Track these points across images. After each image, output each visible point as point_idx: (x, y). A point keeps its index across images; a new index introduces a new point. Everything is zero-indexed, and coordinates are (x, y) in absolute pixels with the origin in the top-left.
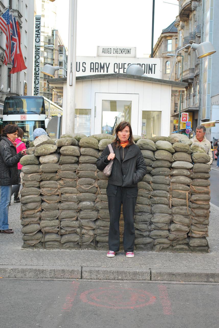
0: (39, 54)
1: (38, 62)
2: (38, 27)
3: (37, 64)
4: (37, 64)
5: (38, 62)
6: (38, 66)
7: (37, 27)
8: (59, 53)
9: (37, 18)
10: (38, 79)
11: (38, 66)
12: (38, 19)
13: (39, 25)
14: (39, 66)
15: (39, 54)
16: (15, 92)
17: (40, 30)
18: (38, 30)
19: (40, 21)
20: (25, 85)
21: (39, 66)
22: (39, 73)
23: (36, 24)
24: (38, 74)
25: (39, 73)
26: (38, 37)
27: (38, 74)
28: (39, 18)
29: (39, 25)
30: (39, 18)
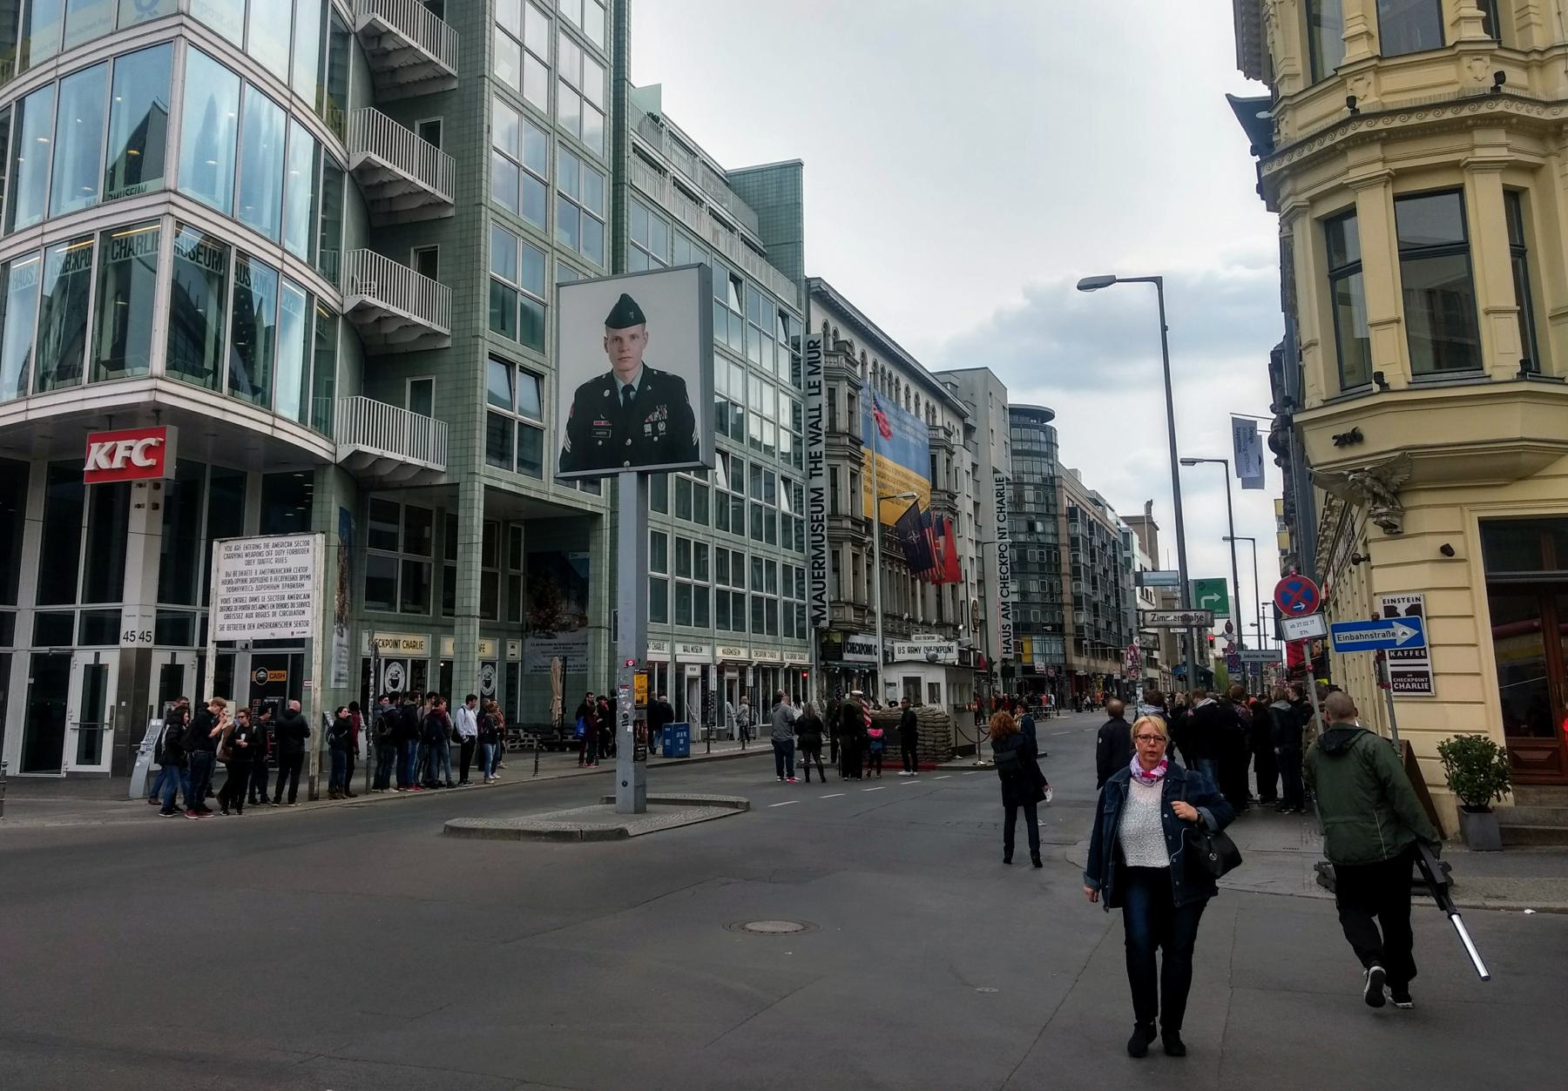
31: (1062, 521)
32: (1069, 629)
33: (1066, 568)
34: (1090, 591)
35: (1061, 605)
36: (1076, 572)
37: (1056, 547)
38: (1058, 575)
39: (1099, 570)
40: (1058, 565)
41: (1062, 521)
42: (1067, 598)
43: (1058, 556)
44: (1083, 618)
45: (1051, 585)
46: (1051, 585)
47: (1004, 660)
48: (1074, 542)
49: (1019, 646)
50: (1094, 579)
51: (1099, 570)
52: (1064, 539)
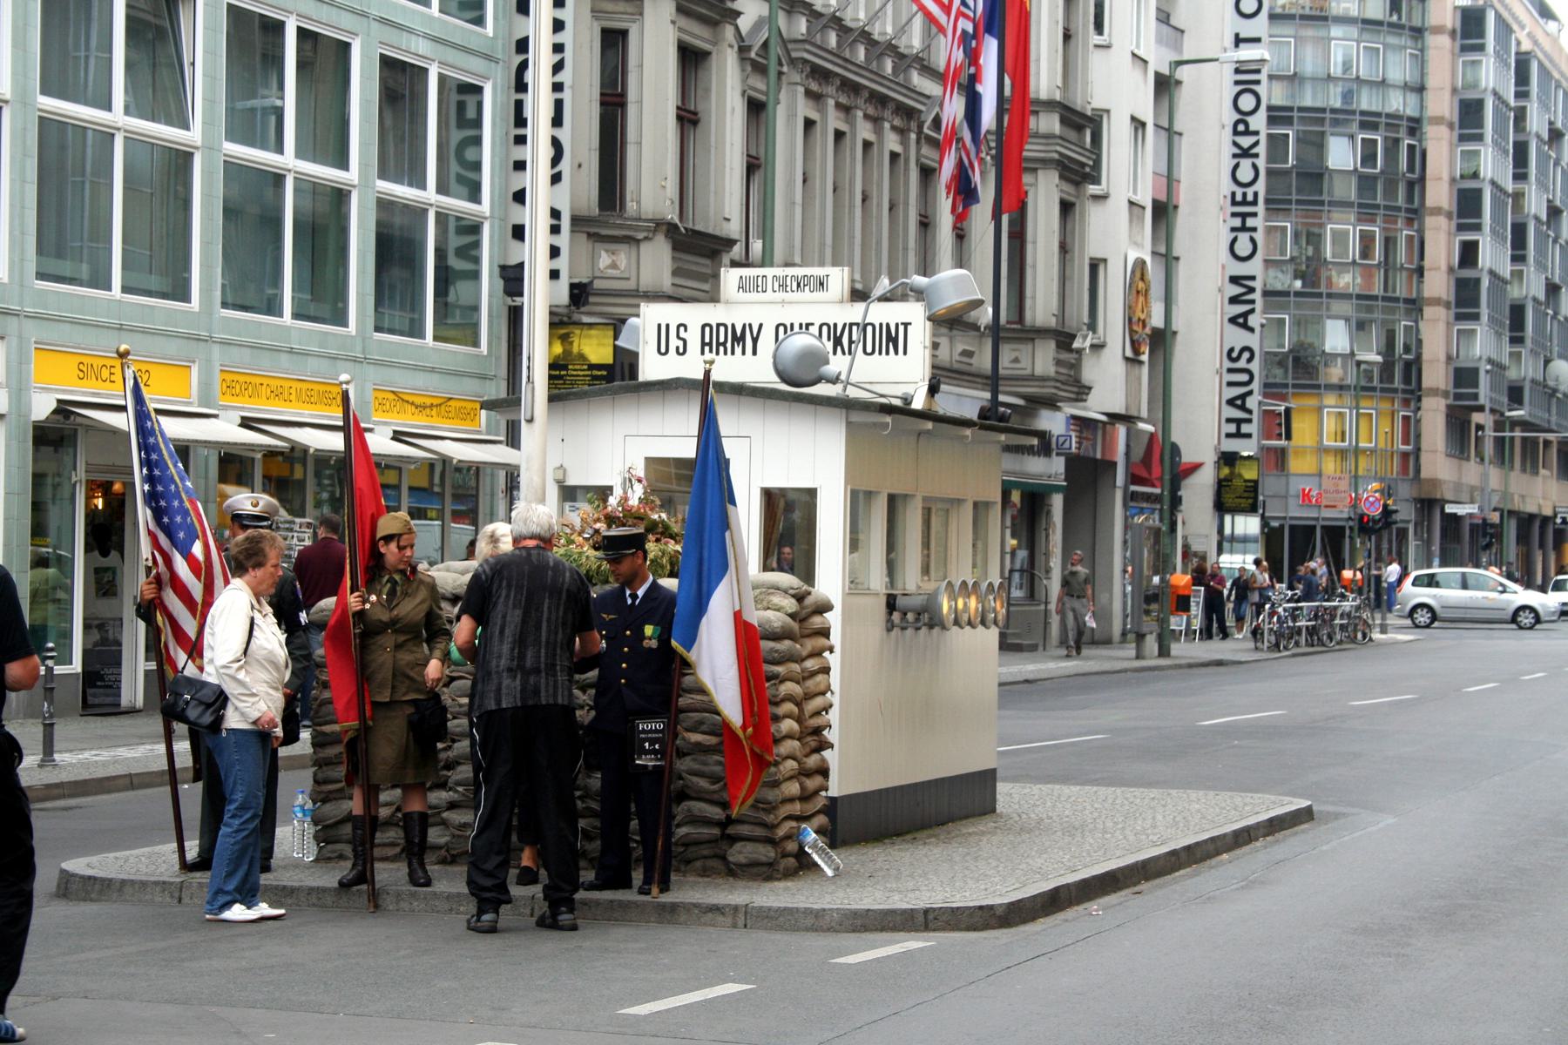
0: (1258, 82)
1: (1252, 128)
3: (1246, 142)
4: (1246, 142)
5: (1252, 128)
6: (1254, 151)
8: (1457, 49)
10: (1254, 229)
11: (1254, 151)
14: (1256, 156)
15: (1258, 82)
16: (1052, 322)
20: (1133, 272)
22: (1256, 194)
24: (1250, 198)
25: (1256, 194)
27: (1250, 198)
31: (1440, 47)
32: (1435, 375)
33: (1439, 194)
34: (1506, 269)
35: (1415, 306)
36: (1468, 204)
37: (1415, 126)
38: (1415, 214)
39: (1535, 205)
40: (1417, 184)
41: (1440, 47)
42: (1437, 284)
43: (1418, 157)
44: (1483, 344)
45: (1389, 243)
46: (1389, 243)
47: (1228, 459)
48: (1470, 112)
49: (1281, 424)
50: (1519, 232)
51: (1535, 205)
52: (1441, 104)
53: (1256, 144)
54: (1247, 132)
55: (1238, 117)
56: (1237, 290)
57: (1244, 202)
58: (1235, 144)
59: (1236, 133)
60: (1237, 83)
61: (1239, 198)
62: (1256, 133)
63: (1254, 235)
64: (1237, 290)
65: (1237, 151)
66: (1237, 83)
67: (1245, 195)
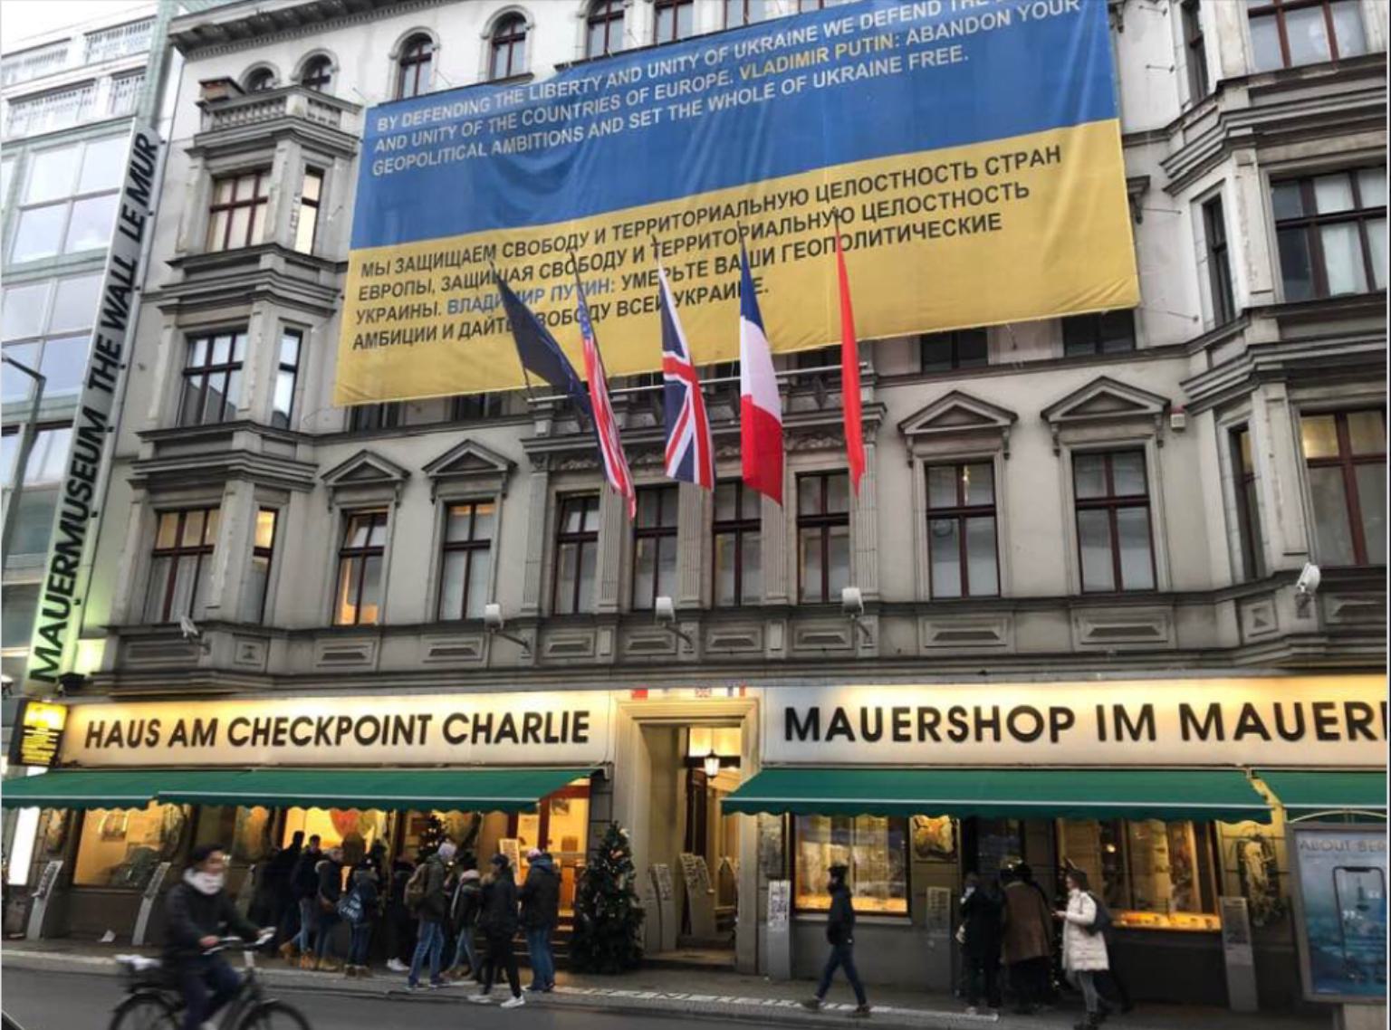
0: (384, 742)
1: (344, 737)
2: (534, 730)
4: (332, 731)
6: (322, 740)
7: (533, 722)
9: (583, 720)
11: (322, 740)
12: (578, 726)
13: (541, 733)
14: (317, 742)
15: (384, 742)
17: (516, 741)
18: (512, 734)
19: (564, 739)
21: (317, 742)
23: (549, 716)
26: (477, 728)
28: (582, 733)
29: (541, 733)
30: (582, 733)
53: (328, 742)
54: (341, 732)
55: (355, 722)
56: (205, 726)
57: (279, 731)
58: (331, 719)
59: (342, 719)
60: (387, 719)
61: (282, 726)
62: (338, 742)
63: (249, 742)
64: (205, 726)
65: (324, 723)
66: (387, 719)
67: (284, 731)
